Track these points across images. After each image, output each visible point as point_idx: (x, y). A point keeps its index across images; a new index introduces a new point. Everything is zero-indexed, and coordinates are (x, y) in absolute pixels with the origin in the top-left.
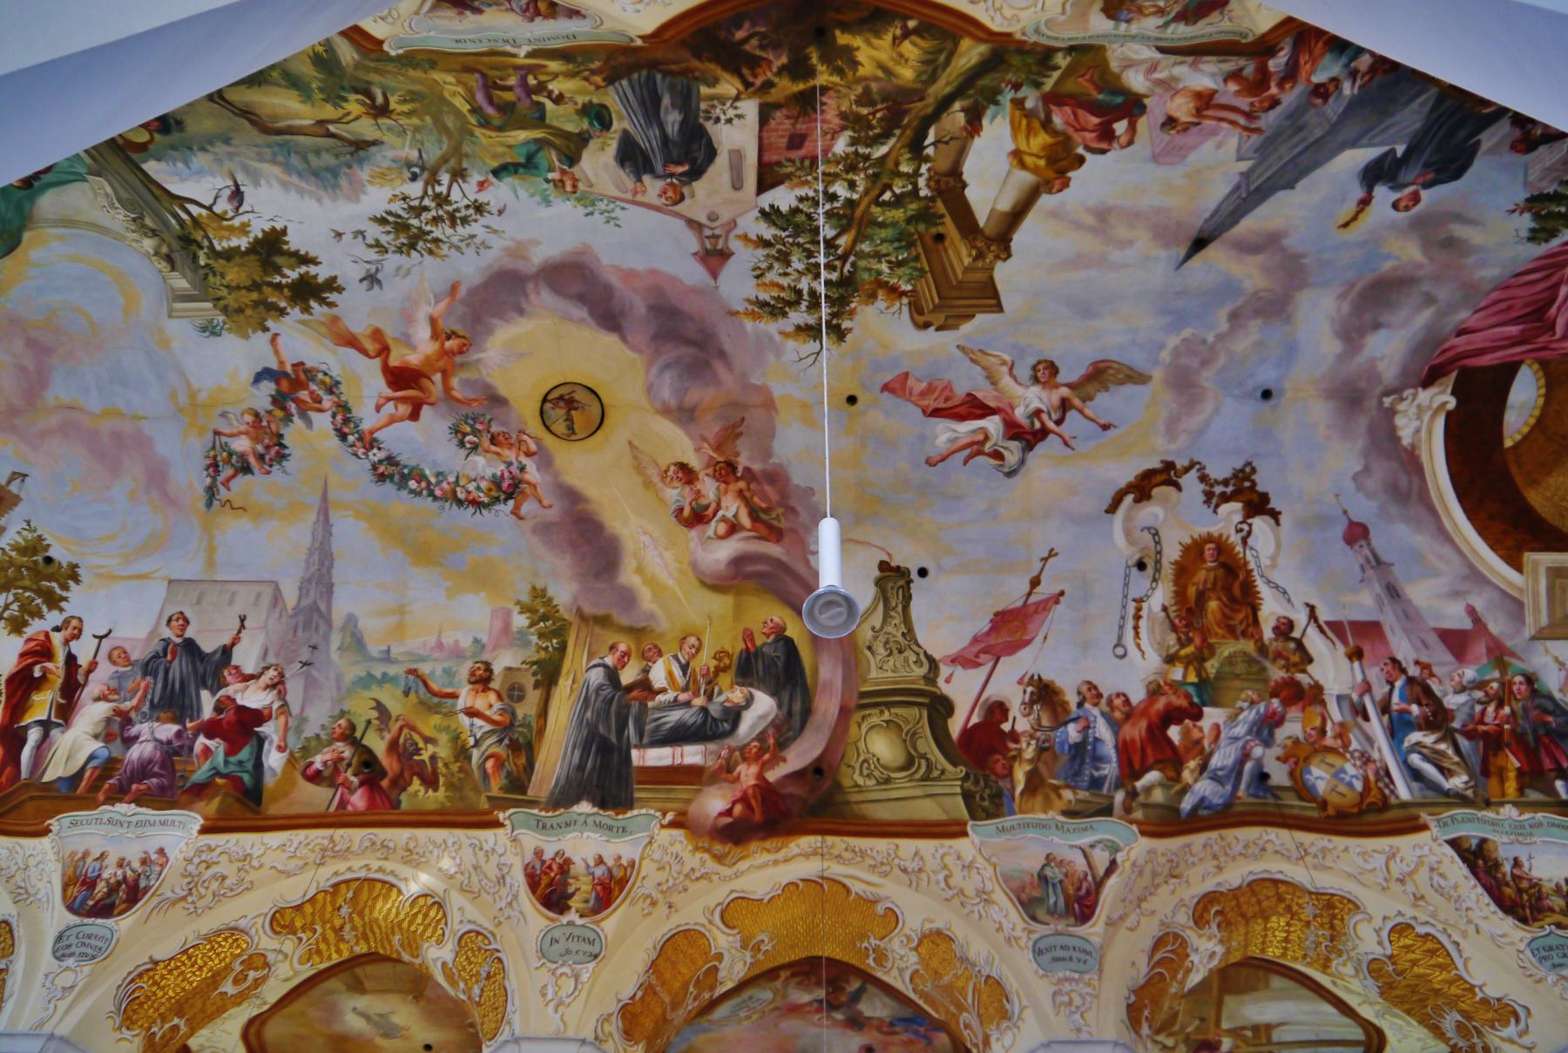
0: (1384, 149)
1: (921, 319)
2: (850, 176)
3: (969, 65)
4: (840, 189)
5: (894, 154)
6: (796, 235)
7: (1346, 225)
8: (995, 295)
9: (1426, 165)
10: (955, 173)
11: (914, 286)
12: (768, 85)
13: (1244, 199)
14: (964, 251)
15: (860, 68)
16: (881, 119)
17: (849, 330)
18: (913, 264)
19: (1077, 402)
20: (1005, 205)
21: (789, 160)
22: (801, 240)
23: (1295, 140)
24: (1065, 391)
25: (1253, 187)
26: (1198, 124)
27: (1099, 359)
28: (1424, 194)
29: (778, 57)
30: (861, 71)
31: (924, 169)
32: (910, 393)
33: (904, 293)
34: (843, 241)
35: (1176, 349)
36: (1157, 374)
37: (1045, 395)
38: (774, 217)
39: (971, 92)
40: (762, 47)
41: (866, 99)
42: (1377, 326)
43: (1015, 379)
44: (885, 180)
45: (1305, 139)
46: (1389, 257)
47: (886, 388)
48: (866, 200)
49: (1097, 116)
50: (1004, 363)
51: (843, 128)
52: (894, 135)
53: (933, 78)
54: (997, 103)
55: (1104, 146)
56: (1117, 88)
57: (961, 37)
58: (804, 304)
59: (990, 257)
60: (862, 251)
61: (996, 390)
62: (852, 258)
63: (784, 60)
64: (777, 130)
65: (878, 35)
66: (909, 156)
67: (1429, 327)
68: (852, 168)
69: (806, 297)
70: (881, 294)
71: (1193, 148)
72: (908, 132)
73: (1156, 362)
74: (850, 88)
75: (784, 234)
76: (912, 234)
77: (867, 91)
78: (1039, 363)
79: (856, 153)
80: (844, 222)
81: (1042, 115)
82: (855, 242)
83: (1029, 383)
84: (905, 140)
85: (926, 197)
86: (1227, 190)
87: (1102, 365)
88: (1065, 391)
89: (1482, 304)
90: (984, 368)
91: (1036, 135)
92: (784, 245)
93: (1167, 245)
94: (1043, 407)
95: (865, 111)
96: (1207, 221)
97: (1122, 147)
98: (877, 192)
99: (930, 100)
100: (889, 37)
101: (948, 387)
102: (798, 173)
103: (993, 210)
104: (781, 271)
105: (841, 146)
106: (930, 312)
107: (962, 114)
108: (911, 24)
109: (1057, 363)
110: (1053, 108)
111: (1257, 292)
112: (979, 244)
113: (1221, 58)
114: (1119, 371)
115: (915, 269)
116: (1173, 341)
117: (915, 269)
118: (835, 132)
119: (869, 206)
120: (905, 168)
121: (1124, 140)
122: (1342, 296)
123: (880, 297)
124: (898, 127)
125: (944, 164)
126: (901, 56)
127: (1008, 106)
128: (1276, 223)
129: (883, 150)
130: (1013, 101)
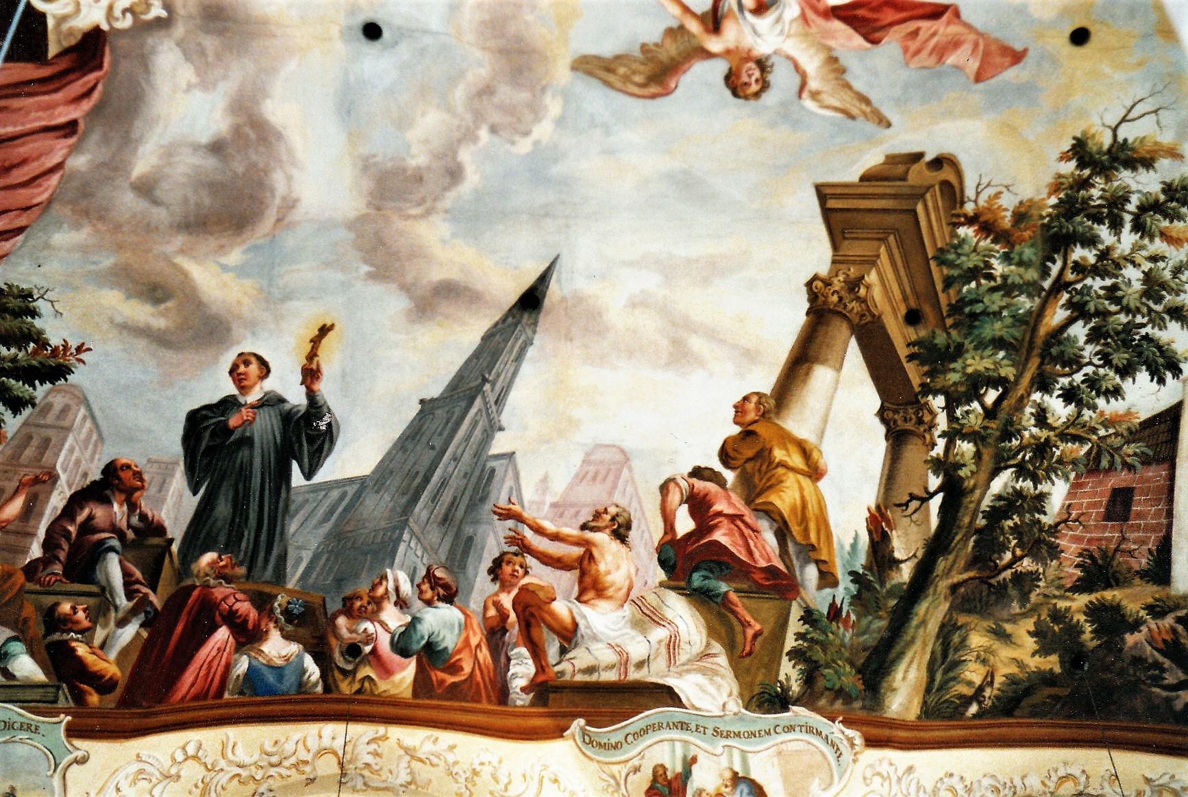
0: (321, 476)
1: (947, 174)
2: (1043, 434)
3: (902, 667)
4: (1060, 411)
5: (983, 476)
6: (1129, 328)
7: (324, 330)
8: (827, 213)
9: (248, 442)
10: (897, 438)
11: (954, 235)
12: (1157, 610)
13: (485, 380)
14: (877, 293)
15: (1032, 628)
16: (1004, 548)
17: (1064, 157)
18: (955, 272)
19: (694, 27)
20: (821, 376)
21: (1130, 467)
22: (1123, 318)
23: (447, 497)
24: (714, 45)
25: (478, 402)
26: (584, 527)
27: (659, 101)
28: (230, 389)
29: (1136, 644)
30: (1029, 624)
31: (939, 449)
32: (976, 45)
33: (971, 221)
34: (1058, 315)
35: (538, 119)
36: (562, 74)
37: (748, 41)
38: (1161, 360)
39: (892, 603)
40: (1157, 665)
41: (1024, 582)
42: (217, 148)
43: (797, 67)
44: (993, 424)
45: (434, 498)
46: (241, 271)
47: (1017, 57)
48: (1021, 391)
49: (716, 544)
50: (815, 95)
51: (1054, 529)
52: (987, 515)
53: (947, 631)
54: (856, 577)
55: (700, 485)
56: (702, 598)
57: (919, 718)
58: (1132, 207)
59: (838, 284)
60: (1030, 296)
61: (830, 49)
62: (1047, 284)
63: (1130, 639)
64: (1147, 528)
65: (1012, 680)
66: (963, 473)
67: (128, 142)
68: (1042, 449)
69: (1128, 218)
70: (1006, 221)
71: (580, 478)
72: (967, 520)
73: (566, 95)
74: (1045, 596)
75: (1148, 330)
76: (955, 326)
77: (1024, 598)
78: (757, 95)
79: (1036, 480)
80: (1054, 351)
81: (791, 548)
82: (1040, 313)
83: (774, 59)
84: (969, 501)
85: (935, 393)
86: (514, 397)
87: (653, 89)
88: (714, 45)
89: (54, 180)
90: (848, 86)
91: (793, 509)
92: (1150, 310)
93: (579, 299)
94: (749, 16)
95: (1027, 564)
96: (528, 343)
97: (672, 480)
98: (1005, 403)
99: (943, 585)
100: (999, 680)
101: (910, 54)
102: (1117, 442)
103: (839, 368)
104: (1161, 264)
105: (1058, 492)
106: (928, 188)
107: (898, 555)
108: (974, 709)
109: (728, 93)
110: (782, 567)
111: (428, 213)
112: (854, 306)
113: (594, 678)
114: (626, 79)
115: (951, 265)
116: (543, 130)
117: (951, 265)
118: (1065, 521)
119: (1018, 377)
120: (966, 448)
121: (675, 497)
122: (290, 204)
123: (1009, 214)
124: (979, 531)
125: (913, 454)
126: (984, 662)
127: (840, 573)
128: (428, 335)
129: (999, 484)
130: (835, 584)
